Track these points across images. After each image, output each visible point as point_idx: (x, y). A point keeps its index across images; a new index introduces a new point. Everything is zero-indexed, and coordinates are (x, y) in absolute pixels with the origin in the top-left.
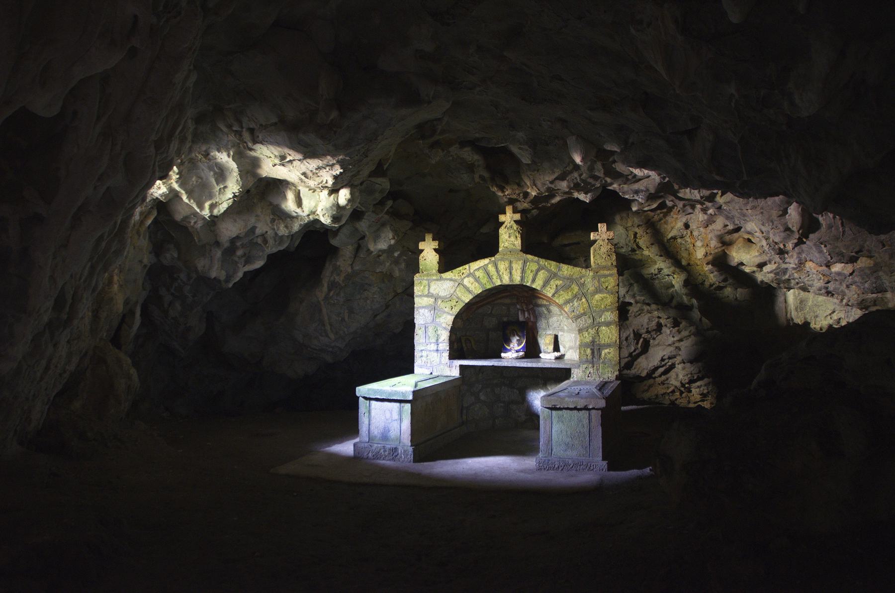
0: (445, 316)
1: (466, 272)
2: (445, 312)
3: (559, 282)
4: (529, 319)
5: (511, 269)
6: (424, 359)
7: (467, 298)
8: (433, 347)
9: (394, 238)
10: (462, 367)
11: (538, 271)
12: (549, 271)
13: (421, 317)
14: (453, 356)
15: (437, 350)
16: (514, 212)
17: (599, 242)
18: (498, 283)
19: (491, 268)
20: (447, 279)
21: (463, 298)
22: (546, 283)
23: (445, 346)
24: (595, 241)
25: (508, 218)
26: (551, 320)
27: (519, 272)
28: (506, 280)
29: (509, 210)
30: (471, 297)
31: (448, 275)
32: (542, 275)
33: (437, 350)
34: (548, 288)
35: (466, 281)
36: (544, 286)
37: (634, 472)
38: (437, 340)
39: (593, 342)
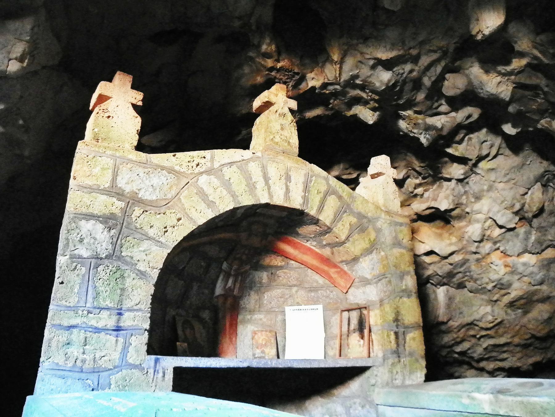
0: (146, 245)
1: (206, 164)
2: (149, 238)
4: (231, 290)
5: (288, 178)
6: (75, 351)
8: (107, 320)
9: (21, 59)
10: (178, 371)
11: (327, 194)
12: (340, 197)
15: (118, 329)
18: (264, 200)
20: (163, 168)
21: (194, 214)
22: (337, 217)
23: (139, 319)
26: (267, 296)
27: (301, 187)
30: (210, 215)
32: (332, 203)
33: (118, 329)
34: (340, 225)
38: (120, 302)
39: (396, 320)
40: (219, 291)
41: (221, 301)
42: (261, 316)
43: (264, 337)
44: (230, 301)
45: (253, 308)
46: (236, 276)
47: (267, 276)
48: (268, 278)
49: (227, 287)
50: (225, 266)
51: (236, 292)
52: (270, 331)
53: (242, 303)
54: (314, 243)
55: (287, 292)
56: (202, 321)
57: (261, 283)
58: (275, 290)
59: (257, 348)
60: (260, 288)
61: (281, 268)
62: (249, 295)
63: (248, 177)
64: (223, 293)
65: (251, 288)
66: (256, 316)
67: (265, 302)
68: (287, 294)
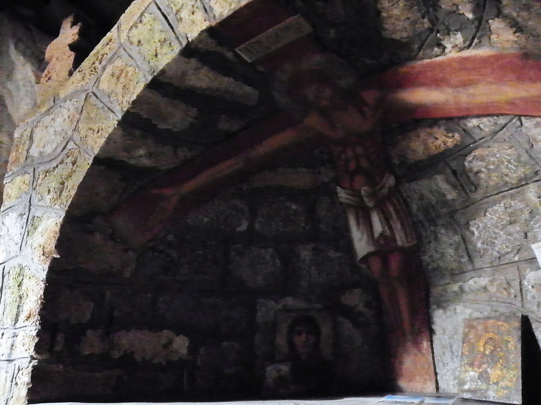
40: (362, 245)
41: (376, 265)
42: (483, 281)
43: (491, 335)
44: (395, 263)
45: (454, 265)
46: (380, 207)
47: (448, 182)
48: (454, 187)
49: (376, 235)
50: (343, 195)
51: (400, 239)
52: (507, 318)
53: (426, 258)
54: (459, 38)
55: (517, 204)
56: (349, 313)
57: (446, 203)
58: (490, 210)
59: (472, 365)
60: (456, 216)
61: (461, 151)
62: (437, 239)
64: (371, 249)
65: (433, 222)
66: (471, 282)
67: (479, 245)
68: (521, 210)
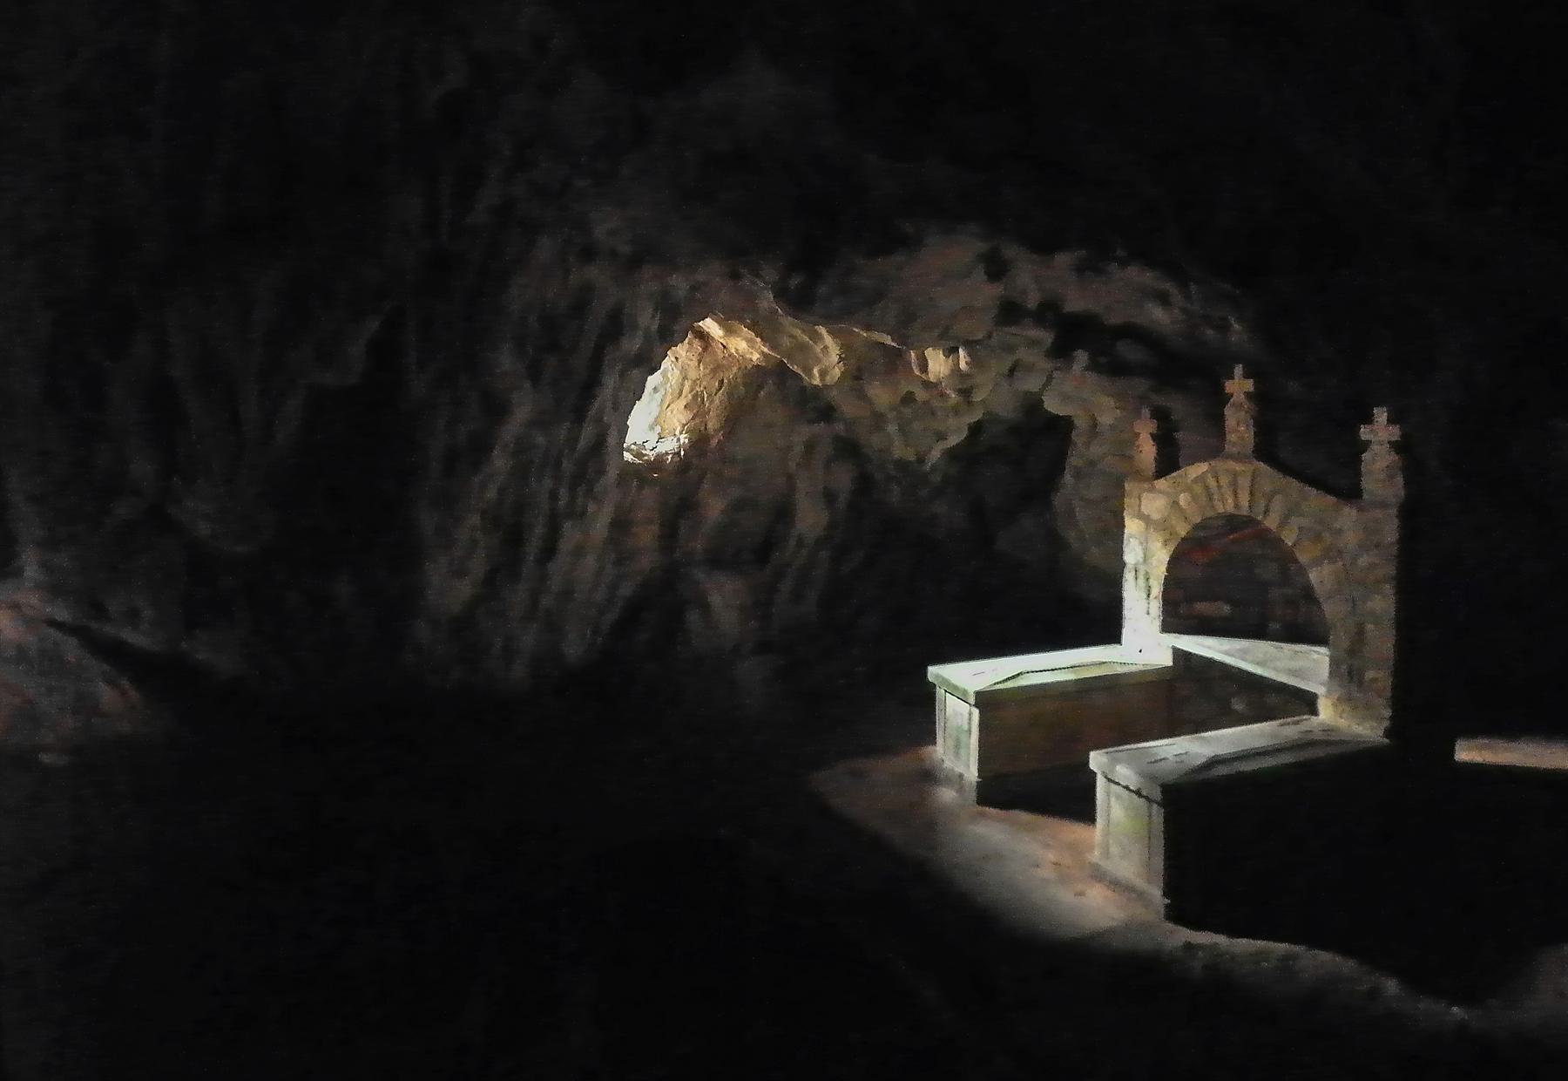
3: (1304, 522)
7: (1183, 530)
13: (1132, 554)
14: (1167, 628)
16: (1246, 376)
17: (1375, 447)
18: (1221, 510)
19: (1212, 483)
24: (1368, 443)
25: (1239, 386)
28: (1229, 506)
29: (1238, 370)
31: (1161, 484)
32: (1278, 506)
35: (1183, 499)
36: (1283, 523)
37: (1221, 940)
63: (1207, 488)
